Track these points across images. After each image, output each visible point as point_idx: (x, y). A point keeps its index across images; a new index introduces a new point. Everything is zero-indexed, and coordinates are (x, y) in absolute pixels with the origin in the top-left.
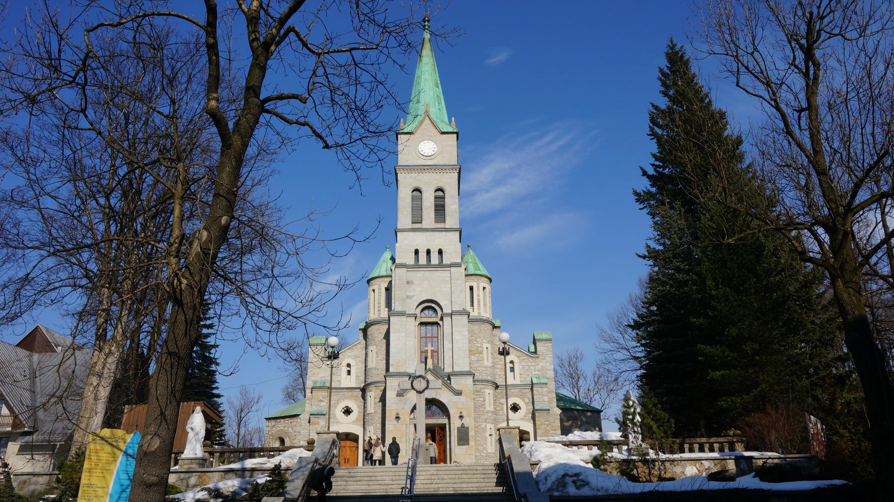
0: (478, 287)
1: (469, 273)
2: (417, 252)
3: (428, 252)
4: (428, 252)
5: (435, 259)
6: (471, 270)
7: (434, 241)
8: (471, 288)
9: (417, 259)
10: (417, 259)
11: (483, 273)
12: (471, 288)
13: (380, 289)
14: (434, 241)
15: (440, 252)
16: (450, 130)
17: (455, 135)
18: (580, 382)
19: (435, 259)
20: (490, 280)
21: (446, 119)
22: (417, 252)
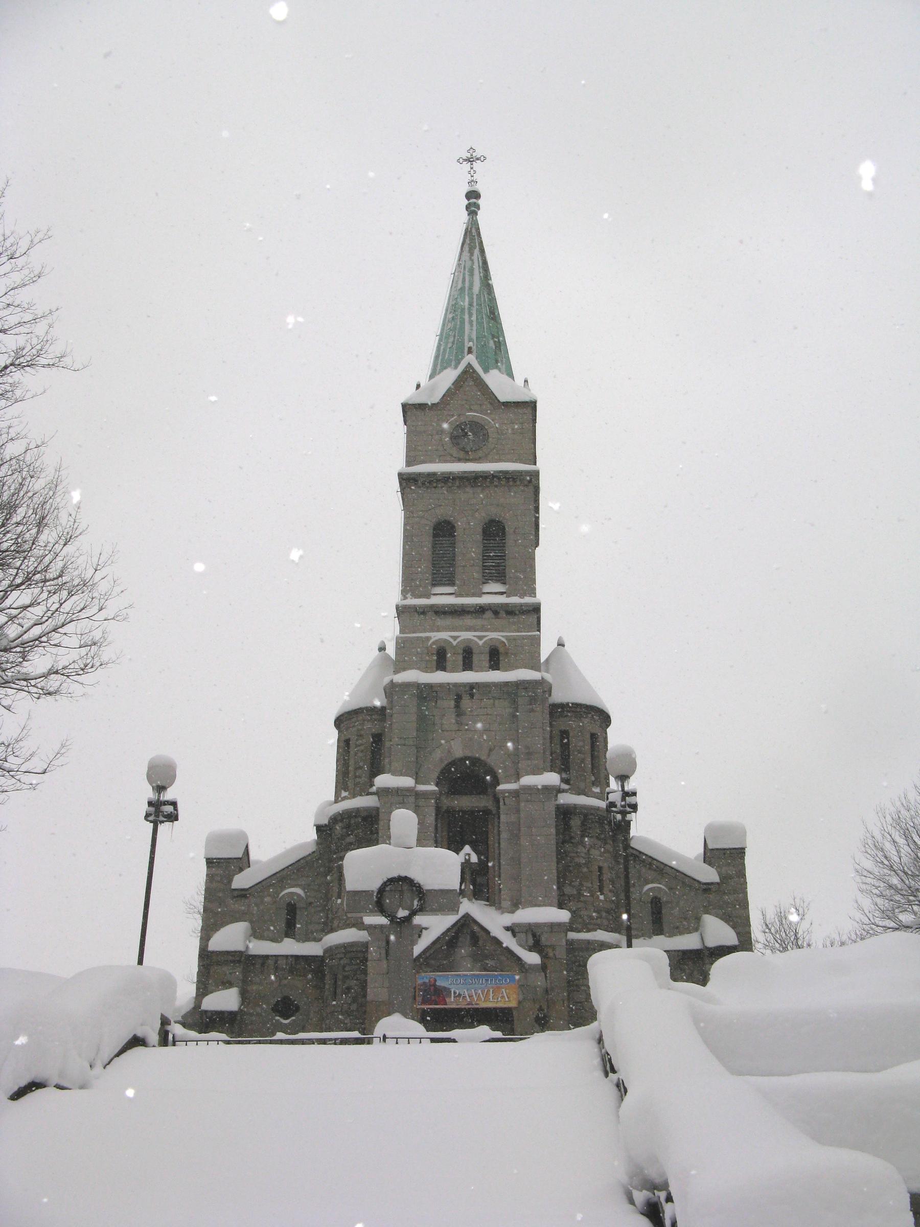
13: (360, 736)
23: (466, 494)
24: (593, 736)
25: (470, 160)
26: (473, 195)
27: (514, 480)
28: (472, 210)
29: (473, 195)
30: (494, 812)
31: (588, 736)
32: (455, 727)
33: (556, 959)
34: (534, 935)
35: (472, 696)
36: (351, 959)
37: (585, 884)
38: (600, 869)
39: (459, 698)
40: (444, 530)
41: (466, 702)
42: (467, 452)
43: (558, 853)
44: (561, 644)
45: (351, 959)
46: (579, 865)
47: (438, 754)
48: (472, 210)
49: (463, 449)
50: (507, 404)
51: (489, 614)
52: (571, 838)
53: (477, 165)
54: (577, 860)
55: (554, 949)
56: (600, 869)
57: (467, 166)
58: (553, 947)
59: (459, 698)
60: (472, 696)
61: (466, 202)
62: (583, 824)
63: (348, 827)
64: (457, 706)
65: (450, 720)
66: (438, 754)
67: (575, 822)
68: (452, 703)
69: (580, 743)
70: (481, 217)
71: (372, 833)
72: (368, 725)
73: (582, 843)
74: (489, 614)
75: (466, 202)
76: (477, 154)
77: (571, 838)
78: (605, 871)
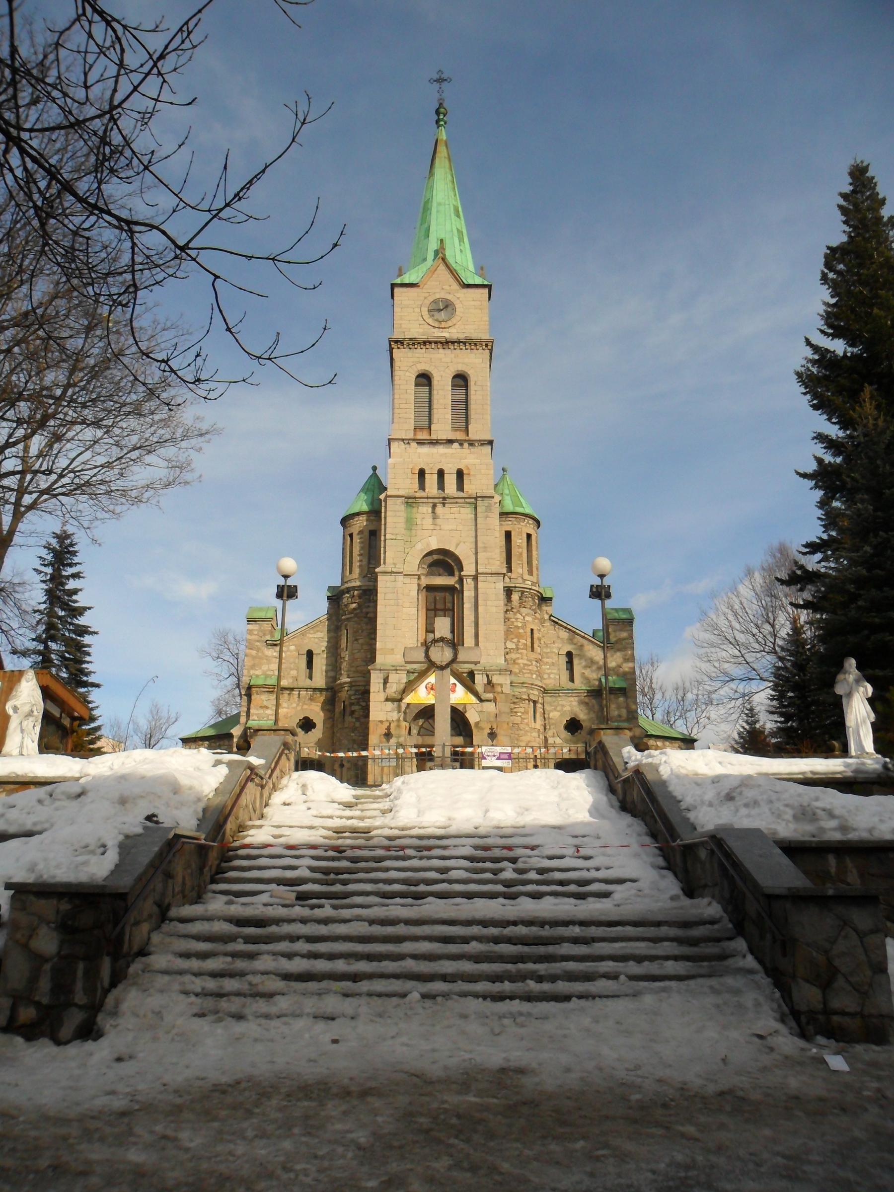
0: (520, 533)
1: (506, 510)
2: (422, 473)
3: (441, 473)
4: (441, 473)
6: (509, 507)
7: (449, 458)
8: (508, 535)
9: (422, 486)
10: (422, 486)
11: (528, 510)
12: (508, 535)
14: (449, 458)
15: (460, 474)
16: (478, 281)
17: (486, 291)
18: (656, 701)
20: (538, 523)
21: (471, 267)
22: (422, 473)
23: (442, 354)
24: (529, 536)
25: (440, 80)
31: (525, 536)
32: (432, 527)
34: (488, 676)
35: (444, 504)
38: (532, 630)
39: (434, 506)
41: (439, 509)
43: (505, 618)
45: (357, 691)
47: (419, 546)
49: (437, 320)
50: (469, 286)
53: (445, 85)
54: (515, 624)
56: (532, 630)
57: (436, 86)
59: (434, 506)
60: (444, 504)
62: (520, 598)
64: (433, 512)
65: (429, 521)
66: (419, 546)
67: (515, 597)
68: (430, 510)
71: (370, 601)
73: (519, 612)
74: (456, 445)
75: (436, 118)
76: (445, 76)
78: (535, 632)
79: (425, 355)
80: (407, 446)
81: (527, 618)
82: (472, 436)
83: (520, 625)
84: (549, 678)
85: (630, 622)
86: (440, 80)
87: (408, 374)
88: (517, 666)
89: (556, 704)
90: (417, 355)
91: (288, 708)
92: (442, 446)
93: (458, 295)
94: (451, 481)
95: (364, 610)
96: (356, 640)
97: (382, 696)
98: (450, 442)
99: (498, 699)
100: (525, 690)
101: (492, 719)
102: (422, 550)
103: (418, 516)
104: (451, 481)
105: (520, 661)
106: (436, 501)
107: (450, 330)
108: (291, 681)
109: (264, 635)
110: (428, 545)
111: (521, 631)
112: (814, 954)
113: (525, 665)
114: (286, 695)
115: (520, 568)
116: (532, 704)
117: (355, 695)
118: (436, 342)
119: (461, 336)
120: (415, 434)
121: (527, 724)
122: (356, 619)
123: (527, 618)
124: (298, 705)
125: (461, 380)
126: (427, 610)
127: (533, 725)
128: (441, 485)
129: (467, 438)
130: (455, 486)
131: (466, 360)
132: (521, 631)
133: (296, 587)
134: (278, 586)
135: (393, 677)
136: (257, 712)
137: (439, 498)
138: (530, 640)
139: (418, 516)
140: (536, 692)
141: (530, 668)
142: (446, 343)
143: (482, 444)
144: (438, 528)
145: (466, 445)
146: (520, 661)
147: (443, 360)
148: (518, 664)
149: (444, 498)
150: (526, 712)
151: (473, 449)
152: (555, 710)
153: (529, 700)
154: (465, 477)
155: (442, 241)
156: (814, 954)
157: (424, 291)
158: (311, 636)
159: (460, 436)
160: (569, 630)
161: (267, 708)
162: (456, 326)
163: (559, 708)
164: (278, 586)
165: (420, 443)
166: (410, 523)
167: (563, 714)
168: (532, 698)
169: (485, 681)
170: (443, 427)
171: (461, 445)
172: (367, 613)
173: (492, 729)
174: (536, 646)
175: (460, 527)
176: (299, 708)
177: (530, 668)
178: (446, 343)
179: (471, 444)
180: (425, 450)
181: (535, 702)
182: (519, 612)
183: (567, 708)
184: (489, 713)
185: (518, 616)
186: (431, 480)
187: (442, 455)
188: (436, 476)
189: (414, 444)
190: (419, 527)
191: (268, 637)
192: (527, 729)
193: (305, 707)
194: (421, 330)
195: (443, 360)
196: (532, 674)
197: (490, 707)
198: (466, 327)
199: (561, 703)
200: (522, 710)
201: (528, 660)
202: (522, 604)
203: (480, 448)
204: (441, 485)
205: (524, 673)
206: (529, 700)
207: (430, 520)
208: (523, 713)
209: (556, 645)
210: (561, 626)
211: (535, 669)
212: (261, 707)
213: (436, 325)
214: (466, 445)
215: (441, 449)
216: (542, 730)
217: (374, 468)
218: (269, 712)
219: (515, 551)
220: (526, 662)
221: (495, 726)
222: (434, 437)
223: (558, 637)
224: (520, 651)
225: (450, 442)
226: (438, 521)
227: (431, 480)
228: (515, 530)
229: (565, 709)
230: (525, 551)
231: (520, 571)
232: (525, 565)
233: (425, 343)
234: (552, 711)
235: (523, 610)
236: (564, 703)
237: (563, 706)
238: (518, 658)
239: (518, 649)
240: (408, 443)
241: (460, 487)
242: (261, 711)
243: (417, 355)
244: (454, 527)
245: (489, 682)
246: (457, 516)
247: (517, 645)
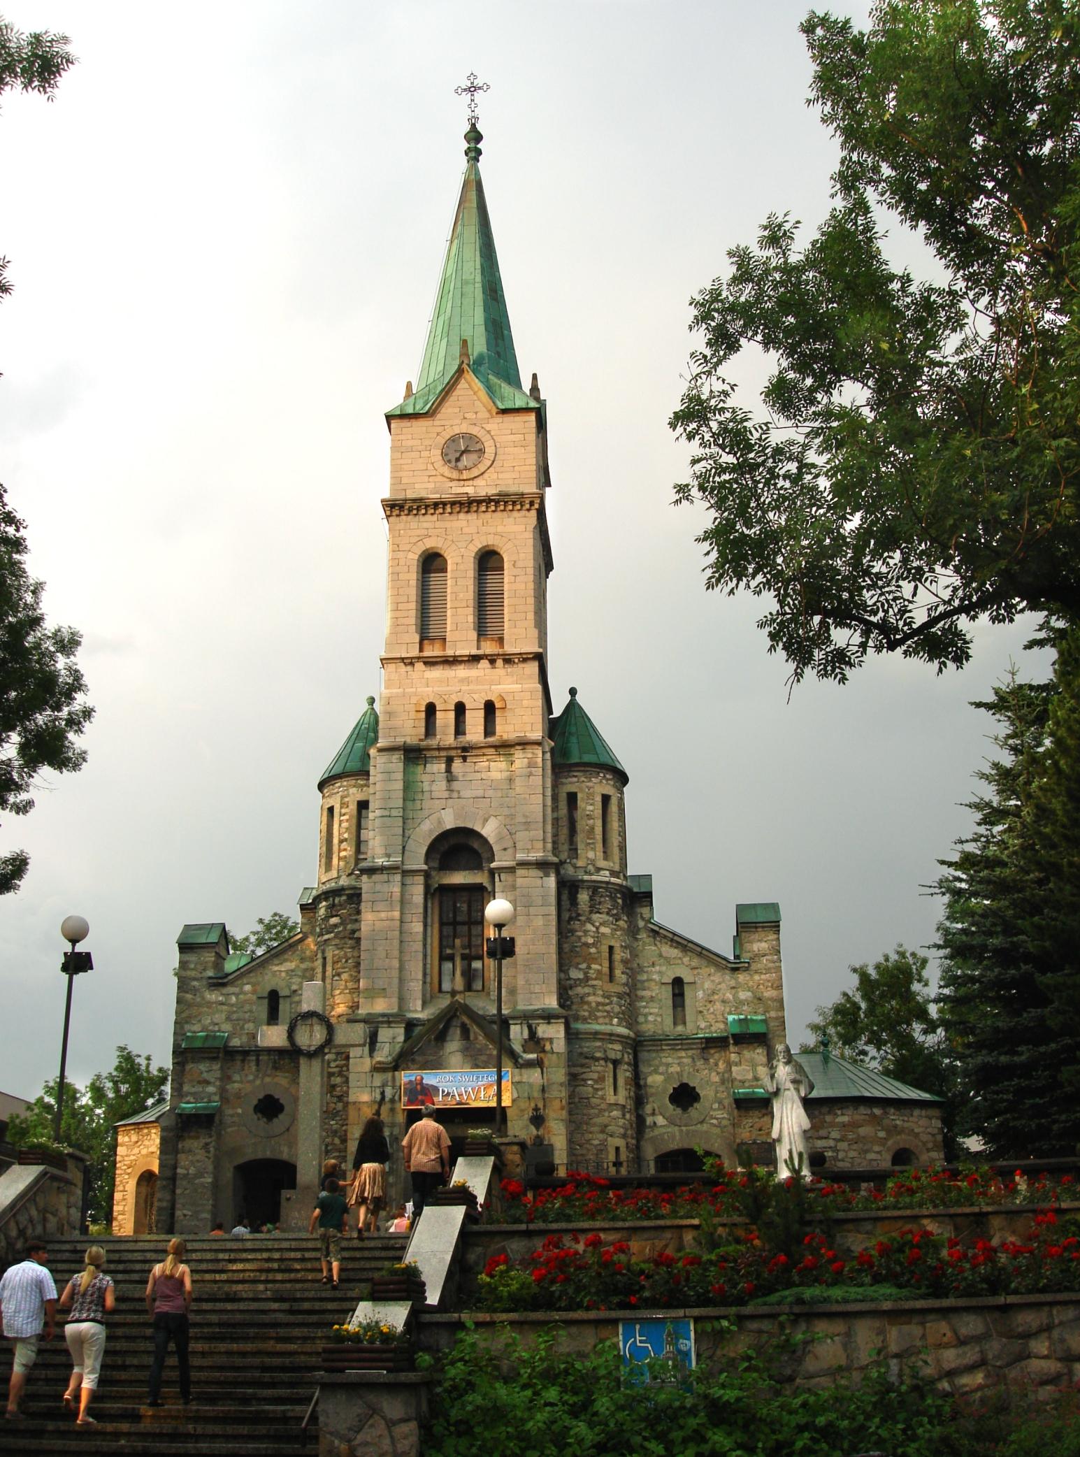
0: (590, 796)
2: (431, 710)
3: (460, 709)
4: (460, 709)
5: (475, 729)
7: (472, 686)
12: (572, 798)
13: (343, 805)
14: (472, 686)
15: (490, 708)
19: (475, 729)
22: (431, 710)
24: (606, 799)
25: (472, 89)
26: (474, 136)
27: (514, 503)
28: (474, 154)
29: (474, 136)
30: (490, 889)
31: (599, 799)
32: (446, 794)
33: (553, 1052)
34: (530, 1027)
35: (464, 759)
36: (337, 1054)
37: (593, 966)
38: (611, 948)
40: (432, 563)
41: (457, 765)
42: (460, 471)
44: (573, 692)
45: (337, 1054)
46: (587, 945)
48: (474, 154)
51: (484, 663)
52: (579, 915)
53: (479, 95)
54: (583, 939)
55: (551, 1043)
56: (611, 948)
57: (466, 97)
58: (551, 1040)
59: (449, 761)
60: (464, 759)
61: (466, 146)
62: (591, 899)
63: (332, 907)
64: (448, 770)
65: (440, 785)
67: (583, 897)
68: (443, 766)
69: (589, 808)
70: (481, 165)
72: (354, 790)
73: (589, 920)
74: (484, 663)
77: (579, 915)
79: (438, 524)
80: (409, 668)
81: (603, 930)
82: (509, 648)
83: (591, 941)
84: (646, 1021)
85: (775, 926)
86: (472, 89)
87: (411, 556)
88: (586, 1007)
89: (656, 1062)
90: (425, 525)
91: (241, 1082)
92: (462, 666)
93: (488, 427)
94: (474, 721)
95: (349, 927)
96: (339, 975)
97: (367, 1063)
98: (475, 659)
99: (546, 1062)
100: (598, 1044)
101: (536, 1094)
102: (431, 831)
103: (425, 778)
104: (474, 721)
105: (591, 998)
106: (453, 753)
107: (476, 482)
108: (245, 1039)
109: (205, 970)
110: (440, 822)
111: (593, 950)
112: (337, 1442)
113: (598, 1004)
114: (239, 1063)
115: (590, 854)
116: (611, 1066)
117: (335, 1060)
118: (453, 504)
119: (492, 491)
120: (421, 650)
121: (603, 1098)
122: (337, 941)
123: (603, 930)
124: (257, 1077)
125: (488, 561)
126: (442, 924)
127: (611, 1099)
128: (459, 729)
129: (501, 651)
130: (481, 729)
131: (500, 529)
132: (593, 950)
133: (88, 955)
134: (65, 954)
135: (384, 1034)
136: (193, 1090)
137: (456, 748)
138: (606, 964)
139: (425, 778)
140: (618, 1047)
141: (608, 1008)
142: (468, 505)
143: (525, 660)
144: (455, 795)
145: (500, 663)
146: (591, 998)
147: (465, 530)
148: (589, 1003)
149: (465, 749)
150: (601, 1079)
151: (510, 669)
152: (656, 1072)
153: (606, 1059)
154: (498, 713)
155: (465, 342)
156: (337, 1442)
157: (437, 423)
158: (276, 968)
159: (489, 648)
160: (678, 943)
161: (208, 1083)
162: (486, 475)
163: (661, 1069)
164: (65, 954)
165: (430, 663)
166: (410, 790)
167: (669, 1078)
168: (612, 1055)
169: (526, 1034)
170: (462, 638)
171: (492, 662)
172: (354, 932)
173: (536, 1109)
174: (618, 972)
175: (490, 793)
176: (258, 1082)
177: (608, 1008)
178: (468, 505)
179: (508, 660)
180: (437, 673)
181: (616, 1063)
182: (589, 920)
183: (675, 1069)
184: (531, 1085)
185: (589, 927)
186: (445, 719)
187: (462, 680)
188: (452, 715)
189: (420, 666)
190: (427, 795)
191: (210, 973)
192: (603, 1106)
193: (268, 1080)
194: (431, 486)
195: (465, 530)
196: (612, 1018)
197: (534, 1076)
198: (501, 476)
199: (664, 1060)
200: (595, 1076)
201: (603, 996)
202: (594, 908)
203: (521, 665)
204: (459, 729)
205: (597, 1018)
206: (606, 1059)
207: (443, 784)
208: (596, 1081)
209: (657, 968)
210: (665, 937)
211: (617, 1009)
212: (199, 1082)
213: (455, 475)
214: (500, 663)
215: (461, 672)
216: (630, 1105)
217: (372, 701)
218: (211, 1089)
219: (581, 825)
220: (600, 999)
221: (540, 1105)
222: (449, 652)
223: (661, 955)
224: (591, 983)
225: (475, 659)
226: (455, 785)
227: (445, 719)
228: (582, 791)
229: (671, 1070)
230: (599, 823)
231: (591, 855)
232: (600, 846)
233: (436, 505)
234: (651, 1073)
235: (595, 916)
236: (670, 1060)
237: (668, 1065)
238: (589, 994)
239: (587, 979)
240: (412, 664)
241: (489, 729)
242: (198, 1089)
243: (425, 525)
244: (480, 793)
245: (532, 1034)
246: (484, 776)
247: (586, 973)
